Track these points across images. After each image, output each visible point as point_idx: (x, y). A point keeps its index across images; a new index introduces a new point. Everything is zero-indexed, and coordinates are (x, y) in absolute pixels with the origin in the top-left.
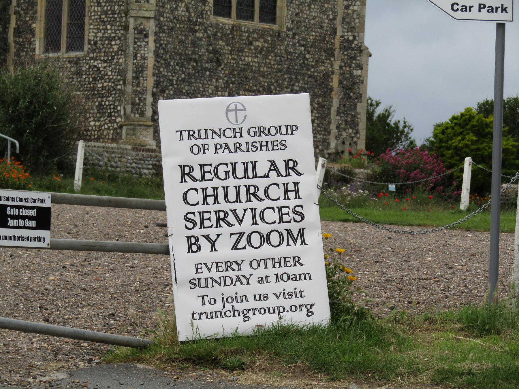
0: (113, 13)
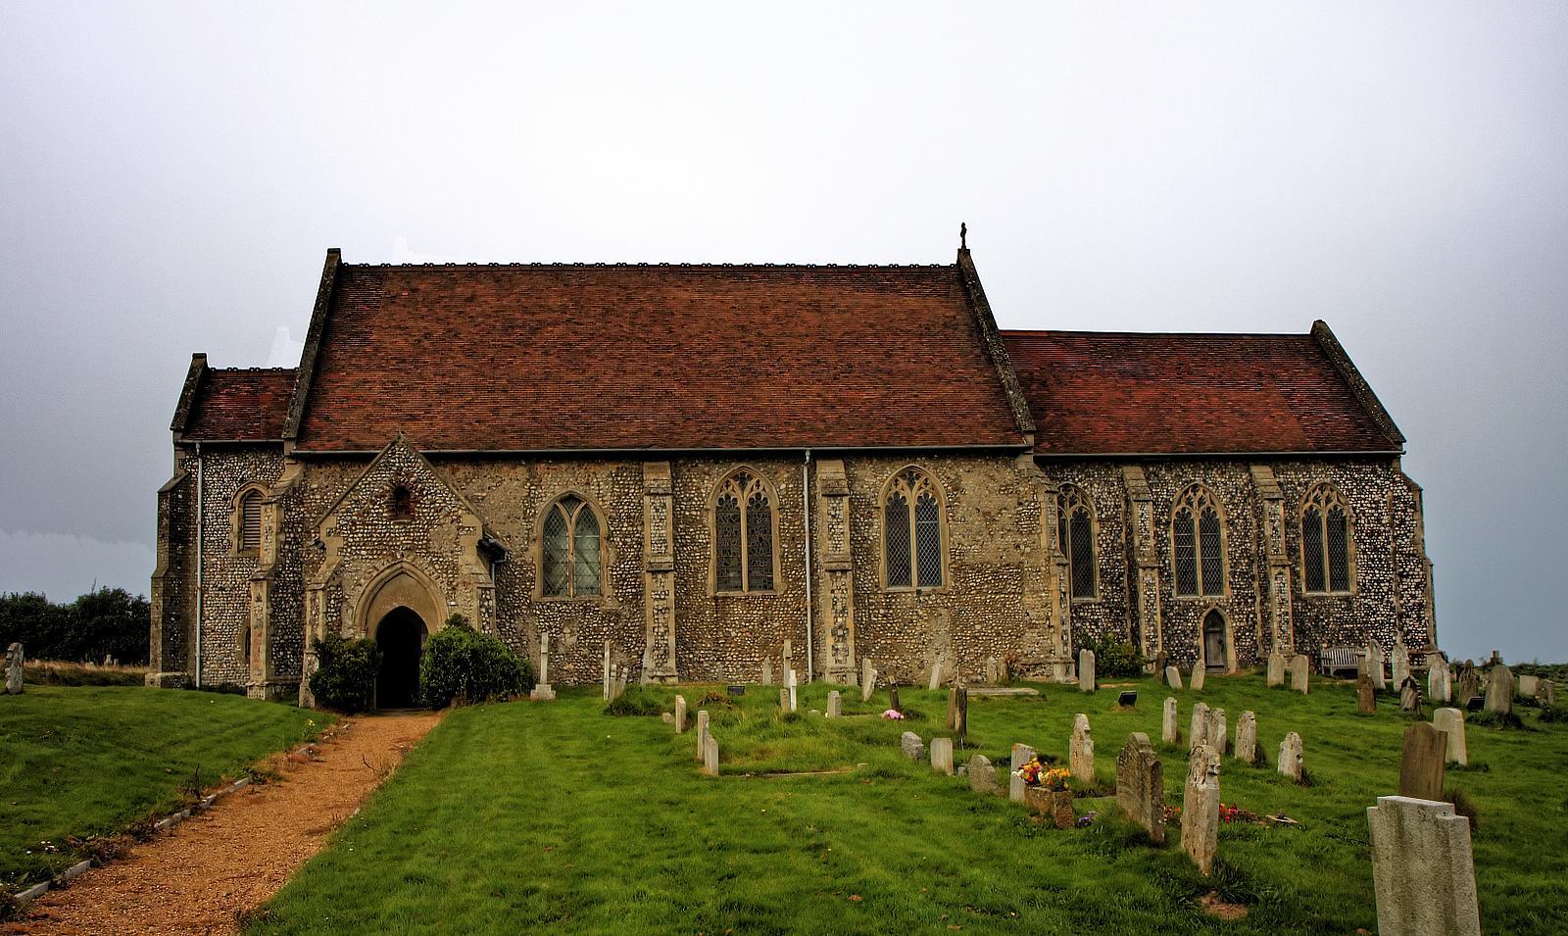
0: (1380, 560)
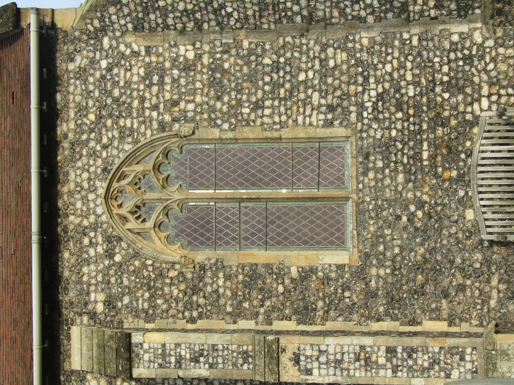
0: (276, 67)
